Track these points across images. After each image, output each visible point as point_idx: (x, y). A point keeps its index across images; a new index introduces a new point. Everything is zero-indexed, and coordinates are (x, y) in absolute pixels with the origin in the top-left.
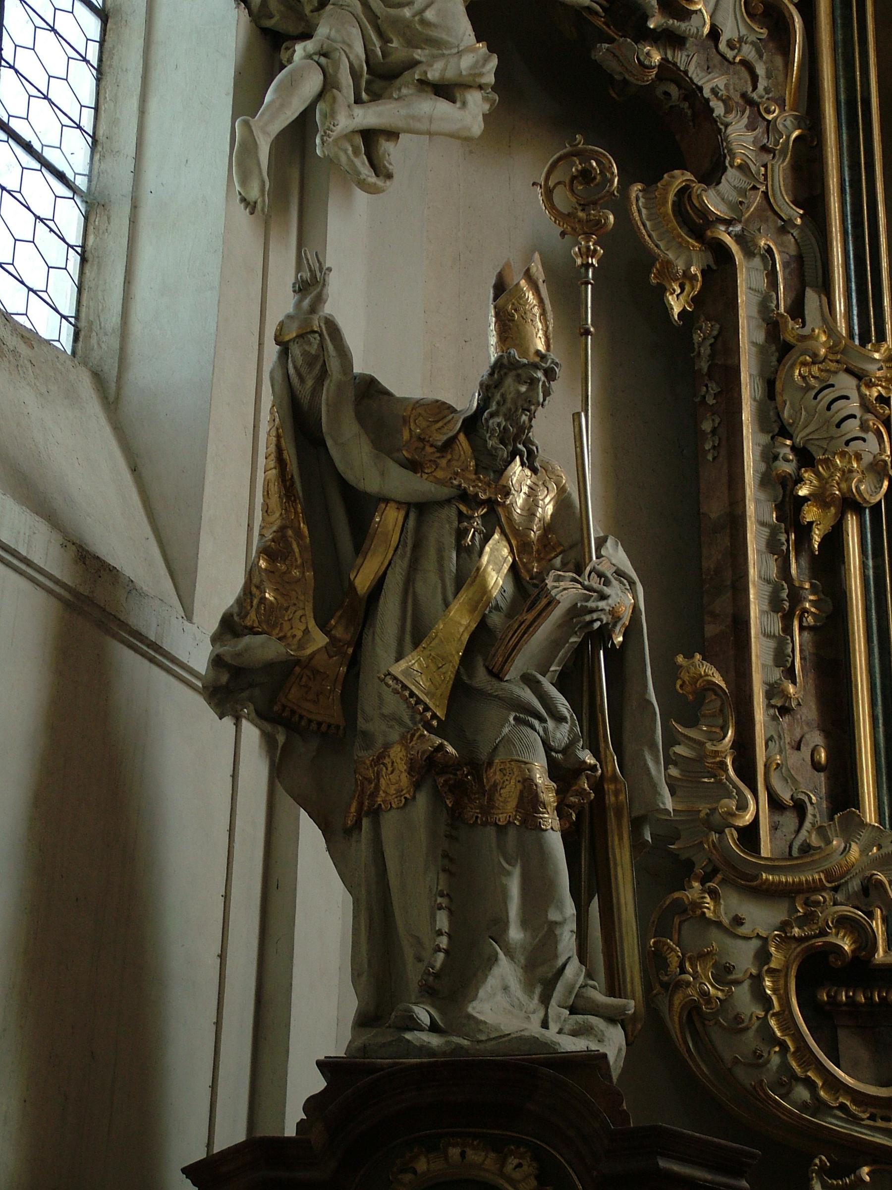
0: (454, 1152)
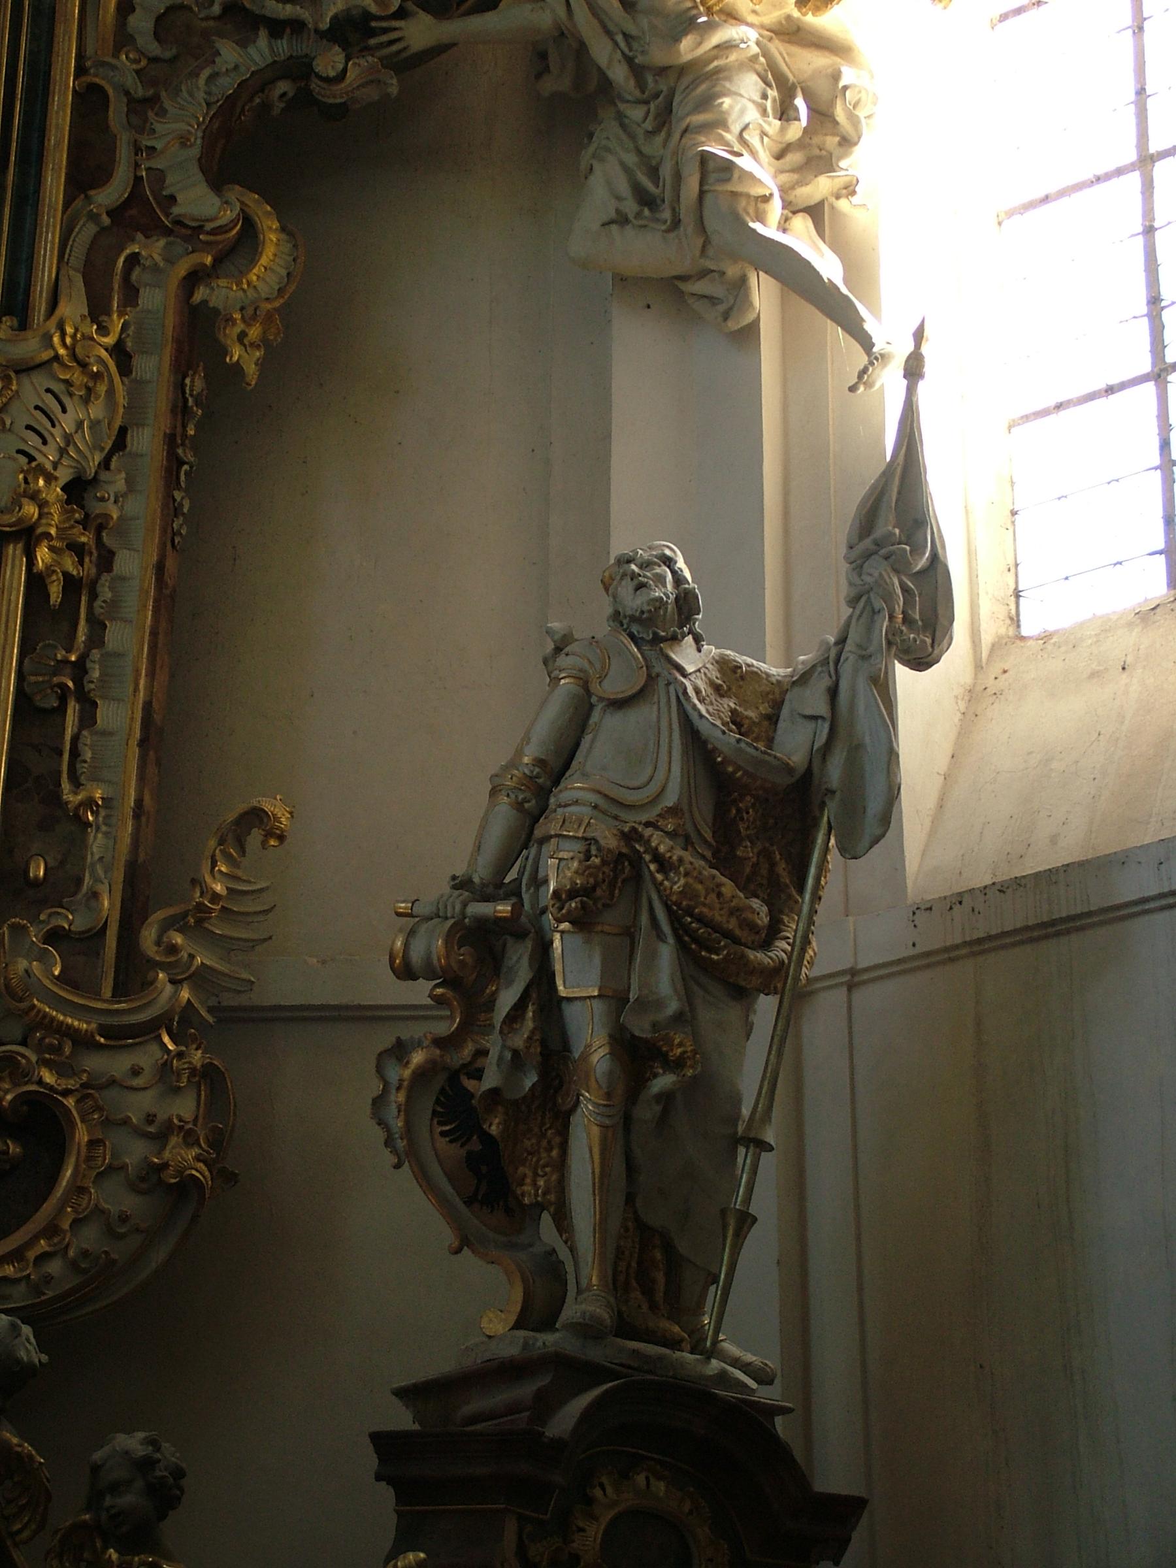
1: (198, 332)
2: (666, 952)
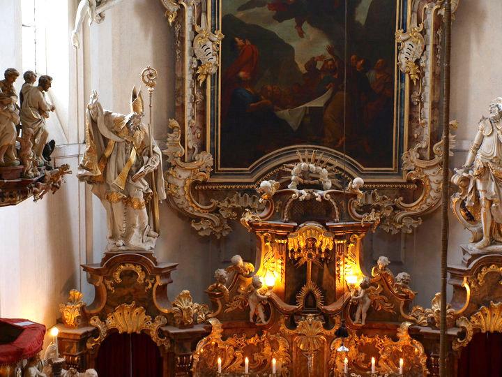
0: (127, 265)
2: (493, 184)
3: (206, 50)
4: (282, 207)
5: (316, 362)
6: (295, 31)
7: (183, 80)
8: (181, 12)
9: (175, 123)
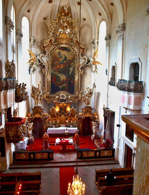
1: (81, 74)
3: (49, 78)
4: (59, 100)
5: (64, 121)
6: (61, 75)
7: (45, 82)
8: (45, 72)
9: (44, 88)
